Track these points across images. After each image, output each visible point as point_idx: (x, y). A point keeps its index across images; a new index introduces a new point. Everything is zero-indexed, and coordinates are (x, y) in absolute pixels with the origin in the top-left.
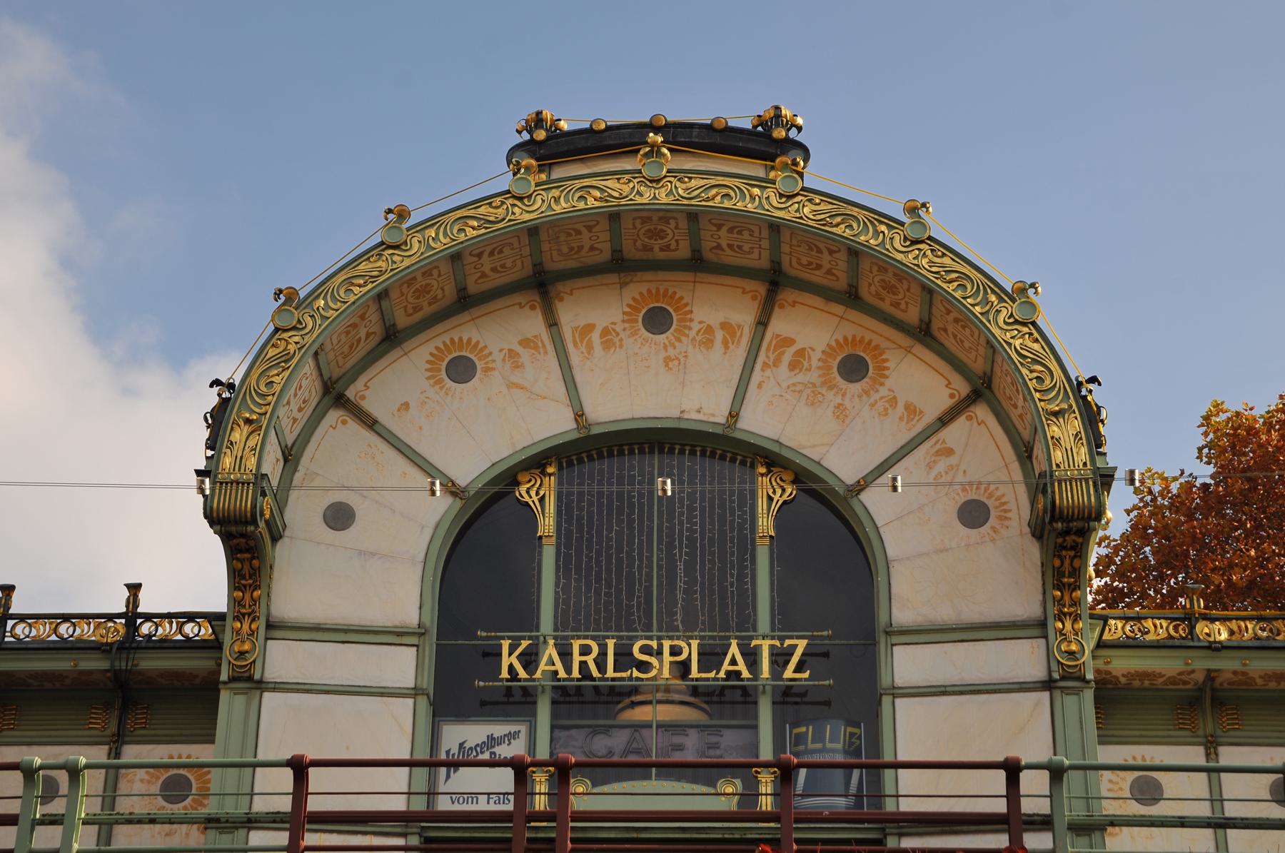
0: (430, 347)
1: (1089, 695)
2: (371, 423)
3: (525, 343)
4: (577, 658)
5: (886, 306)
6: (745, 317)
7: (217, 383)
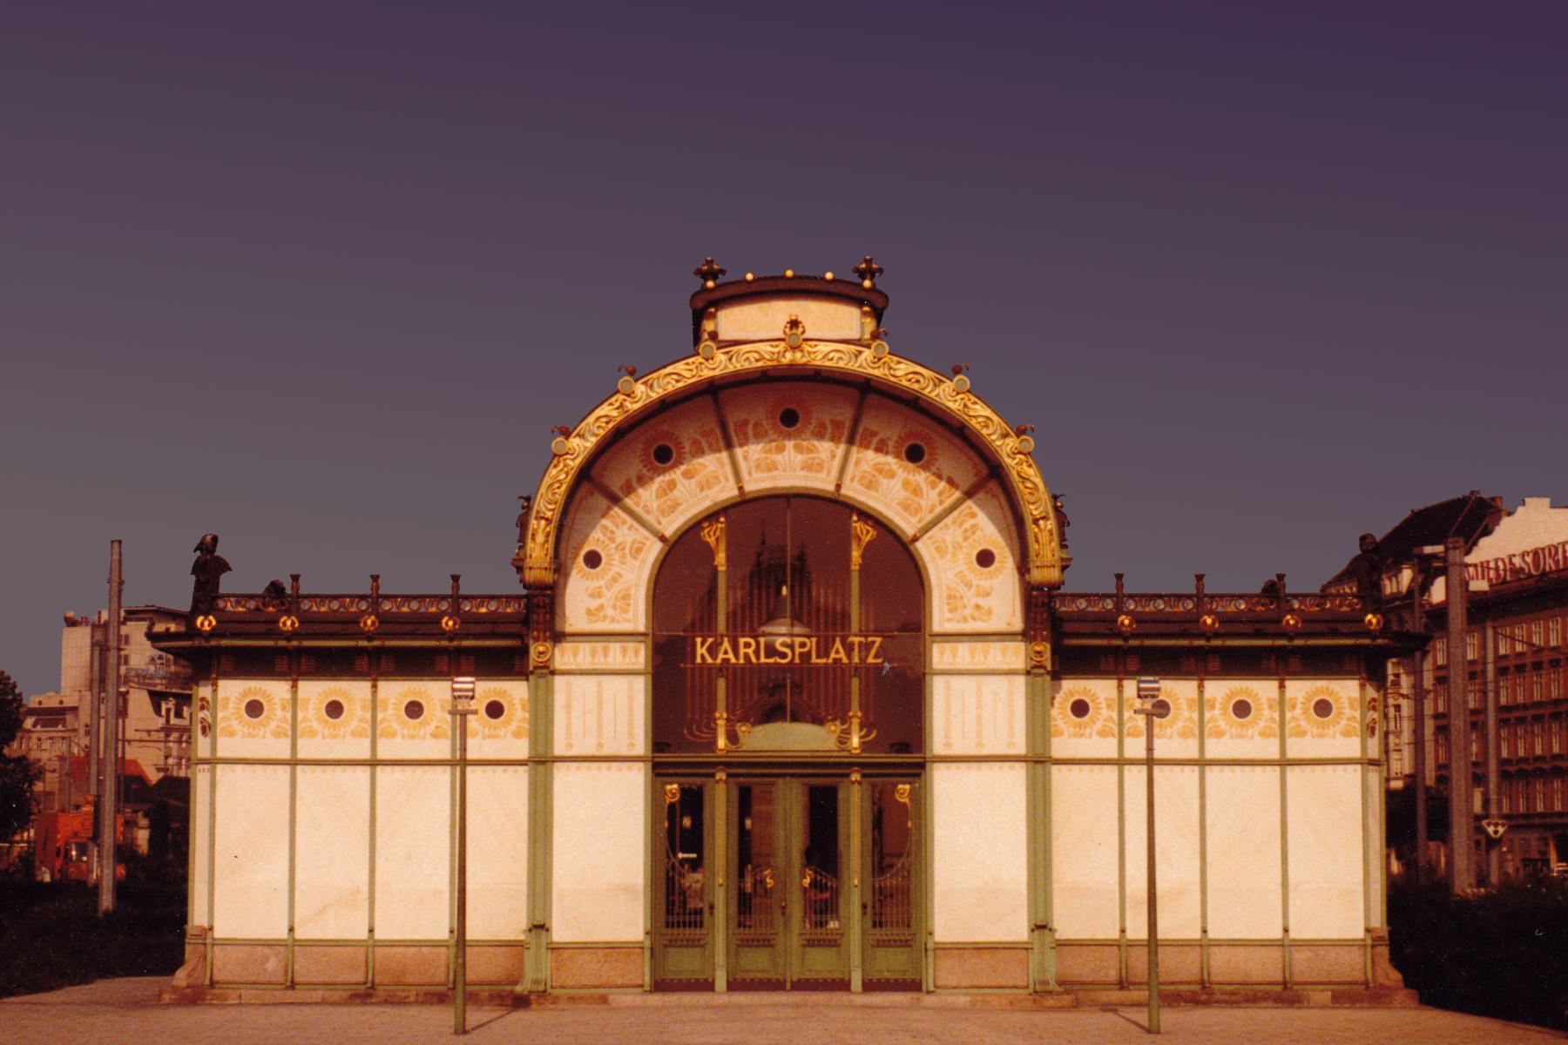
3: (705, 434)
4: (742, 650)
6: (845, 414)
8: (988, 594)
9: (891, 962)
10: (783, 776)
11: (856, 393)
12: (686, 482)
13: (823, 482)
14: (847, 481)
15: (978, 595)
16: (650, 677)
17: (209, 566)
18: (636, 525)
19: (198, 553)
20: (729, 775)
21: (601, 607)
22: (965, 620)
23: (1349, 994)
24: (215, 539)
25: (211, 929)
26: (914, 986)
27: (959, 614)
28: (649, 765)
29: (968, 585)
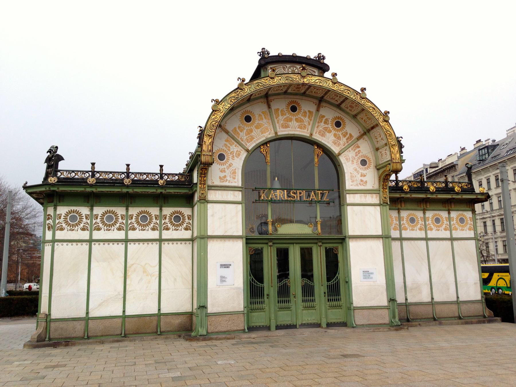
0: (240, 113)
1: (388, 207)
2: (227, 132)
5: (348, 110)
7: (200, 127)
8: (365, 176)
9: (335, 315)
10: (293, 243)
11: (317, 102)
12: (256, 130)
13: (305, 133)
14: (314, 134)
15: (361, 176)
16: (244, 205)
17: (53, 159)
18: (238, 145)
19: (49, 154)
20: (273, 243)
21: (225, 177)
22: (357, 185)
23: (482, 320)
24: (57, 147)
25: (50, 315)
26: (344, 324)
27: (355, 183)
28: (244, 239)
29: (358, 172)
